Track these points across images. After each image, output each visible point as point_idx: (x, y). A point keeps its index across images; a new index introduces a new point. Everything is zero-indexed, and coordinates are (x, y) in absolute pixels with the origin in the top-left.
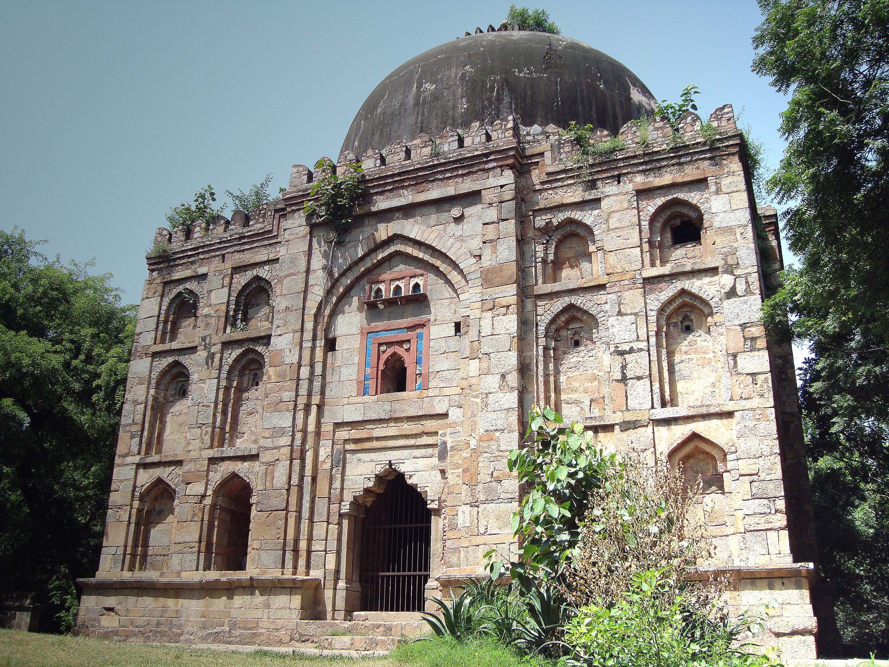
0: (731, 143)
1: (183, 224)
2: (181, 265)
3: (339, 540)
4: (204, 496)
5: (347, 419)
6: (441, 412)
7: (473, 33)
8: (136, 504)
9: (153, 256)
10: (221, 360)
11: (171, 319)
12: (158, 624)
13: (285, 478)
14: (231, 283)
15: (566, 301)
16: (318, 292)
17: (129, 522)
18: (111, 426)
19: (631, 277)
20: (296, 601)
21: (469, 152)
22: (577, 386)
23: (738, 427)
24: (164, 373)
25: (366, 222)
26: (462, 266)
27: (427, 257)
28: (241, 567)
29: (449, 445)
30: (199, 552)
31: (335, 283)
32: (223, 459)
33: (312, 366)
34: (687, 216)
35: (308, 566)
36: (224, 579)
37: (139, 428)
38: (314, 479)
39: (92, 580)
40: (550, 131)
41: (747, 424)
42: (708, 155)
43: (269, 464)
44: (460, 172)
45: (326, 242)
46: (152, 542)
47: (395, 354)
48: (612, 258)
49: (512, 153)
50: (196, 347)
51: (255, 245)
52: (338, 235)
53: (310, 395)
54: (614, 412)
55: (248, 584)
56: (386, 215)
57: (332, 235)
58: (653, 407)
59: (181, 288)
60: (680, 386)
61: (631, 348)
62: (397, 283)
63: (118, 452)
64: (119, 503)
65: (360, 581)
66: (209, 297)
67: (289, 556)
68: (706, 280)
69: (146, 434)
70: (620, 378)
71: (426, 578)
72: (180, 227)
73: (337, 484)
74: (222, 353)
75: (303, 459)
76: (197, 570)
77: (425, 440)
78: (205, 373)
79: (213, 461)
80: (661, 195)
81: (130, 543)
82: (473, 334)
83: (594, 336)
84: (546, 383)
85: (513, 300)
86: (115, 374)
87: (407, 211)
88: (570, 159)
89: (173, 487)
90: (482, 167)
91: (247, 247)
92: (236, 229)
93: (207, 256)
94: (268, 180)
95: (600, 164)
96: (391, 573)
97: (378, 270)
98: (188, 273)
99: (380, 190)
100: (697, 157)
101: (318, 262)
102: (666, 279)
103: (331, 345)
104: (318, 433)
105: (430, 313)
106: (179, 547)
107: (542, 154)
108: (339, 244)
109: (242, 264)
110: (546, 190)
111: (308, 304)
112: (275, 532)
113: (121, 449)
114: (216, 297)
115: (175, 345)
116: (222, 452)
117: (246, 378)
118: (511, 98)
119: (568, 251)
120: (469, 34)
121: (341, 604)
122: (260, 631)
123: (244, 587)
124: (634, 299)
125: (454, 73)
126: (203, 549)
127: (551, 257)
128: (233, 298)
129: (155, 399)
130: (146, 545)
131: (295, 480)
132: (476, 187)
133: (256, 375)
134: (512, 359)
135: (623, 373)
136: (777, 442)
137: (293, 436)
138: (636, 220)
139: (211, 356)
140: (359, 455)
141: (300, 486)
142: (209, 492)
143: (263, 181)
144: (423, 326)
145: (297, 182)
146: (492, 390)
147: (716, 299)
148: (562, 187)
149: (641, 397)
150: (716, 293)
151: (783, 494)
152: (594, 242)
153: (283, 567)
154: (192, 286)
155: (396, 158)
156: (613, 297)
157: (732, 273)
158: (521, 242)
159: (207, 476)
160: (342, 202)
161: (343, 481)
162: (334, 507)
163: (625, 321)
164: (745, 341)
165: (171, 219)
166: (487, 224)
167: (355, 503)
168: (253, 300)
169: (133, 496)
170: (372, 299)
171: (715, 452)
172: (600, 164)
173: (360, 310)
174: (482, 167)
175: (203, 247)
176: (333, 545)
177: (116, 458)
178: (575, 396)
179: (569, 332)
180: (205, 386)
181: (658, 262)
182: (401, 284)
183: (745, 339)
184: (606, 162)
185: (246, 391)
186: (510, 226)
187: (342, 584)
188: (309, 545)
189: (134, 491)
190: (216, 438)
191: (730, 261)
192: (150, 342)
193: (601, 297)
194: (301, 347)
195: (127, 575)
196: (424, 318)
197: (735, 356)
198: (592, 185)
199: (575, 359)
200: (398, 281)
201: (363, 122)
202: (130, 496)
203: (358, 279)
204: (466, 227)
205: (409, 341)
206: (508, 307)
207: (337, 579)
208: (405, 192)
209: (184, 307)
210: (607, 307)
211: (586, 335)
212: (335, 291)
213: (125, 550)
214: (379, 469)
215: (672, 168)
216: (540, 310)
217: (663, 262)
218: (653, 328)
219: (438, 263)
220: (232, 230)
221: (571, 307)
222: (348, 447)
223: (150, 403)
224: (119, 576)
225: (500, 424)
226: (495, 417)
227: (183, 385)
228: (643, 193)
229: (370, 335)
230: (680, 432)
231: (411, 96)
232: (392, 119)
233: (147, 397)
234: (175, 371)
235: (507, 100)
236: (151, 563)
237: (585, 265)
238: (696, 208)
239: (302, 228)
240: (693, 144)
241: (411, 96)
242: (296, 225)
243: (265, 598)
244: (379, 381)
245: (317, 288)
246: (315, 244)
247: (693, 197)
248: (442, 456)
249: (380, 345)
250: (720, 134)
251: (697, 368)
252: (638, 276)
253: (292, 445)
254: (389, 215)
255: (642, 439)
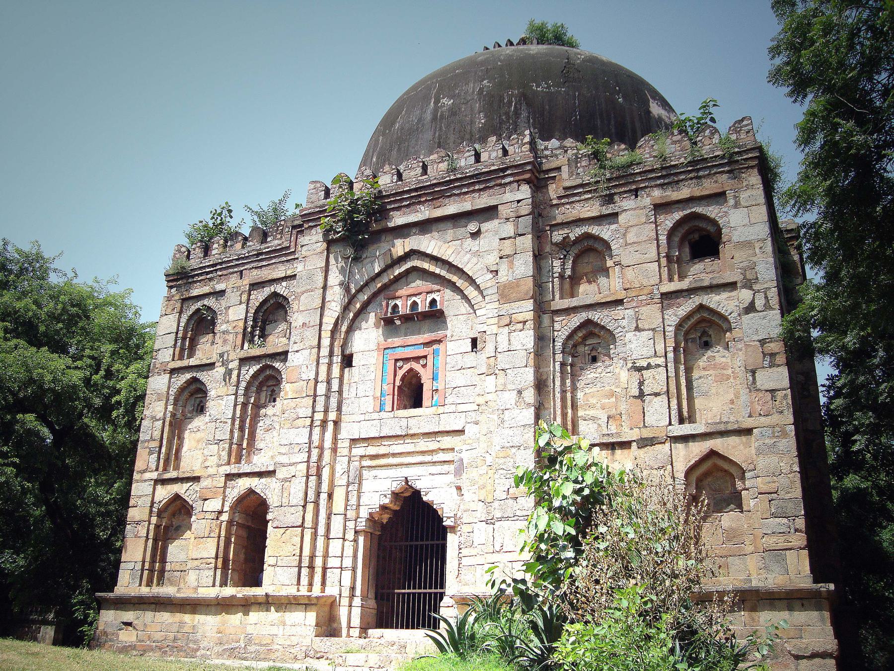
0: (750, 155)
1: (201, 241)
2: (200, 281)
3: (355, 557)
4: (220, 512)
6: (457, 429)
7: (491, 47)
8: (154, 520)
9: (171, 272)
10: (239, 376)
11: (189, 336)
12: (175, 639)
13: (301, 495)
14: (249, 300)
15: (583, 316)
16: (335, 309)
17: (147, 538)
18: (131, 442)
19: (648, 292)
20: (311, 617)
21: (486, 166)
22: (594, 402)
23: (757, 444)
24: (182, 390)
25: (383, 238)
26: (478, 281)
27: (443, 273)
28: (258, 583)
30: (216, 568)
31: (352, 299)
32: (240, 475)
33: (329, 382)
34: (705, 230)
35: (323, 583)
36: (240, 595)
37: (156, 444)
38: (330, 496)
39: (111, 595)
40: (568, 145)
41: (766, 442)
42: (727, 169)
43: (286, 480)
44: (477, 187)
45: (343, 258)
46: (169, 558)
47: (411, 370)
48: (630, 273)
49: (529, 168)
50: (214, 364)
51: (273, 261)
52: (355, 251)
53: (326, 411)
54: (631, 429)
55: (263, 600)
56: (403, 231)
57: (349, 251)
58: (670, 424)
59: (199, 305)
60: (698, 403)
61: (649, 364)
62: (414, 298)
63: (136, 468)
64: (137, 519)
65: (376, 598)
66: (227, 314)
67: (305, 572)
68: (724, 295)
69: (163, 450)
70: (637, 394)
71: (442, 595)
72: (199, 244)
73: (353, 501)
74: (240, 370)
75: (319, 476)
76: (214, 586)
77: (441, 457)
78: (222, 390)
79: (230, 477)
80: (678, 209)
81: (148, 559)
82: (489, 349)
83: (612, 352)
84: (563, 399)
85: (530, 315)
86: (135, 390)
87: (424, 226)
88: (587, 173)
89: (191, 503)
90: (498, 182)
91: (264, 263)
92: (254, 245)
93: (225, 272)
94: (286, 196)
95: (617, 178)
96: (407, 591)
97: (395, 286)
98: (206, 289)
99: (396, 205)
100: (715, 170)
101: (335, 278)
102: (684, 294)
103: (347, 361)
104: (334, 450)
105: (447, 329)
106: (196, 563)
107: (558, 169)
108: (356, 259)
109: (259, 281)
110: (563, 204)
111: (324, 320)
112: (291, 548)
113: (139, 465)
114: (234, 314)
115: (193, 362)
116: (239, 468)
117: (263, 395)
118: (529, 113)
119: (585, 266)
120: (487, 49)
121: (356, 621)
122: (275, 647)
123: (260, 604)
124: (651, 314)
125: (472, 88)
126: (220, 565)
127: (568, 272)
128: (251, 315)
129: (173, 415)
130: (163, 561)
131: (311, 496)
132: (492, 202)
133: (273, 391)
134: (529, 376)
135: (641, 390)
136: (796, 460)
137: (309, 452)
138: (654, 234)
139: (229, 372)
140: (374, 472)
141: (316, 503)
142: (226, 508)
143: (281, 197)
144: (439, 341)
145: (314, 198)
147: (734, 315)
148: (579, 201)
149: (658, 413)
150: (735, 308)
151: (803, 512)
152: (611, 257)
153: (299, 583)
154: (210, 302)
155: (412, 173)
156: (630, 312)
157: (751, 288)
158: (538, 257)
159: (224, 492)
160: (358, 217)
161: (359, 497)
162: (351, 525)
163: (642, 338)
164: (764, 357)
165: (189, 236)
166: (504, 239)
167: (371, 519)
168: (271, 317)
169: (151, 511)
170: (389, 315)
171: (733, 470)
172: (617, 178)
173: (377, 326)
174: (498, 182)
175: (221, 264)
176: (348, 562)
177: (135, 473)
178: (591, 413)
179: (587, 348)
180: (222, 402)
181: (676, 277)
182: (417, 299)
183: (764, 355)
184: (623, 176)
185: (263, 407)
186: (527, 241)
187: (357, 601)
188: (325, 563)
189: (152, 506)
190: (234, 454)
191: (749, 276)
192: (168, 358)
193: (619, 312)
194: (318, 363)
195: (145, 591)
196: (439, 334)
197: (753, 372)
198: (609, 199)
199: (593, 375)
200: (414, 295)
201: (381, 138)
202: (147, 511)
203: (375, 295)
204: (483, 243)
205: (425, 357)
206: (525, 322)
207: (352, 596)
208: (422, 208)
209: (202, 324)
210: (624, 323)
211: (603, 351)
212: (352, 307)
213: (143, 565)
214: (396, 486)
215: (690, 182)
216: (557, 326)
217: (682, 277)
218: (671, 344)
219: (454, 278)
220: (250, 246)
221: (588, 322)
223: (168, 419)
224: (137, 591)
225: (516, 441)
226: (511, 433)
227: (201, 401)
228: (660, 207)
229: (387, 351)
230: (698, 449)
231: (429, 112)
232: (410, 134)
233: (165, 414)
234: (193, 387)
235: (524, 114)
236: (168, 579)
237: (602, 280)
238: (714, 222)
239: (319, 244)
240: (711, 158)
241: (429, 112)
242: (313, 241)
243: (279, 614)
244: (396, 397)
245: (334, 304)
246: (332, 261)
247: (711, 211)
248: (459, 472)
250: (739, 147)
251: (715, 384)
252: (656, 292)
253: (308, 461)
254: (406, 231)
255: (659, 457)
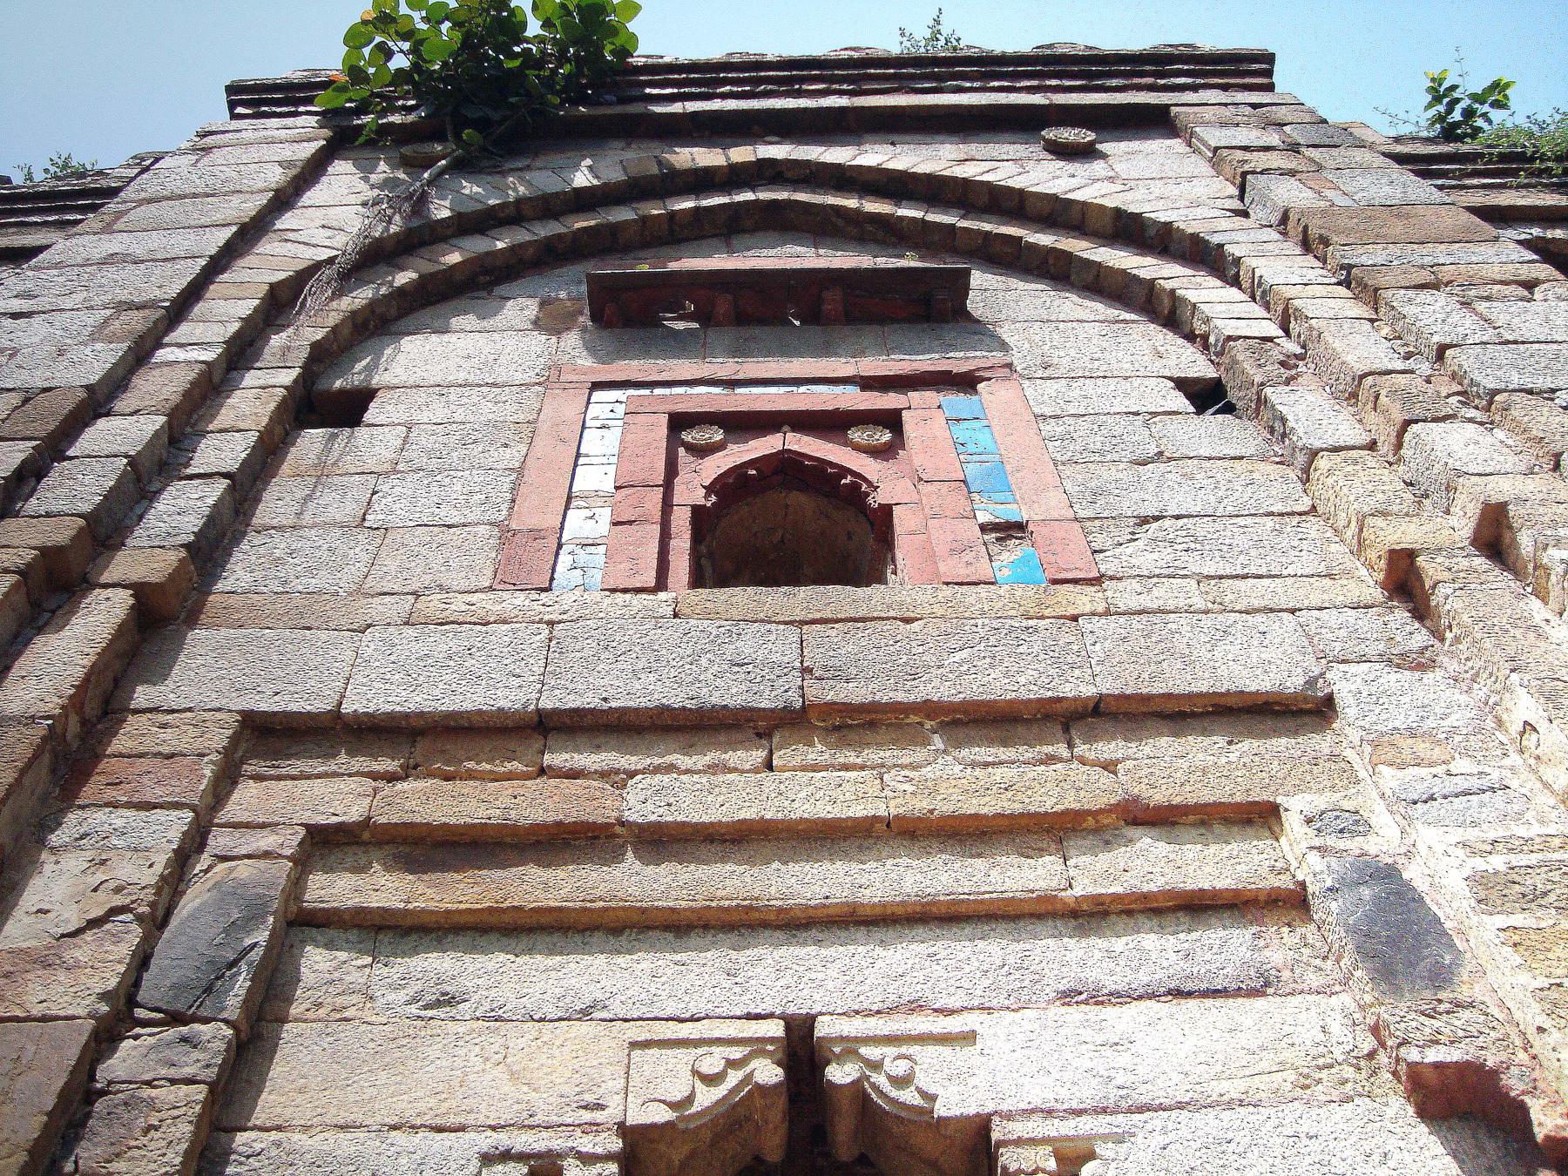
144: (967, 382)
222: (333, 889)
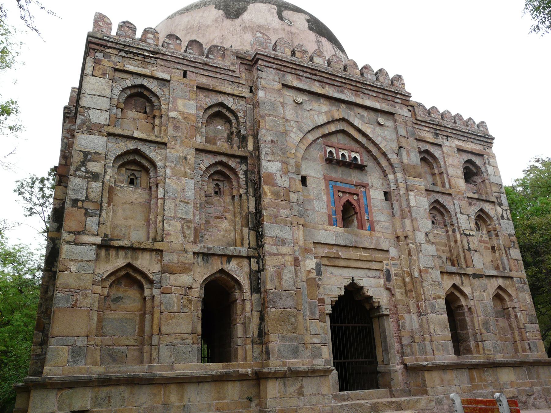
5: (323, 241)
6: (385, 249)
29: (393, 272)
50: (165, 144)
62: (343, 152)
135: (469, 247)
146: (422, 242)
214: (347, 282)
234: (131, 158)
249: (339, 191)
